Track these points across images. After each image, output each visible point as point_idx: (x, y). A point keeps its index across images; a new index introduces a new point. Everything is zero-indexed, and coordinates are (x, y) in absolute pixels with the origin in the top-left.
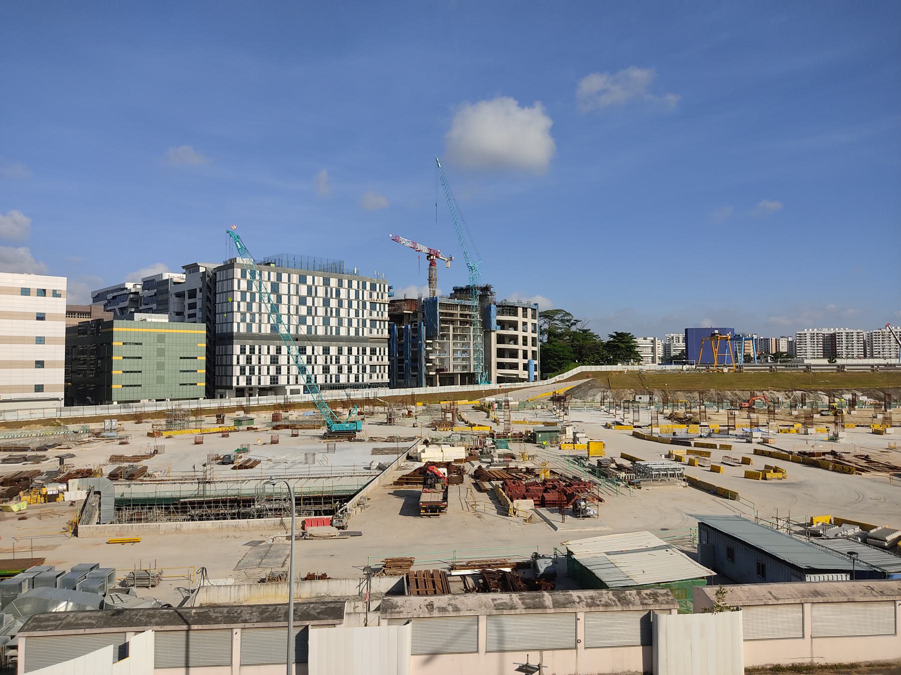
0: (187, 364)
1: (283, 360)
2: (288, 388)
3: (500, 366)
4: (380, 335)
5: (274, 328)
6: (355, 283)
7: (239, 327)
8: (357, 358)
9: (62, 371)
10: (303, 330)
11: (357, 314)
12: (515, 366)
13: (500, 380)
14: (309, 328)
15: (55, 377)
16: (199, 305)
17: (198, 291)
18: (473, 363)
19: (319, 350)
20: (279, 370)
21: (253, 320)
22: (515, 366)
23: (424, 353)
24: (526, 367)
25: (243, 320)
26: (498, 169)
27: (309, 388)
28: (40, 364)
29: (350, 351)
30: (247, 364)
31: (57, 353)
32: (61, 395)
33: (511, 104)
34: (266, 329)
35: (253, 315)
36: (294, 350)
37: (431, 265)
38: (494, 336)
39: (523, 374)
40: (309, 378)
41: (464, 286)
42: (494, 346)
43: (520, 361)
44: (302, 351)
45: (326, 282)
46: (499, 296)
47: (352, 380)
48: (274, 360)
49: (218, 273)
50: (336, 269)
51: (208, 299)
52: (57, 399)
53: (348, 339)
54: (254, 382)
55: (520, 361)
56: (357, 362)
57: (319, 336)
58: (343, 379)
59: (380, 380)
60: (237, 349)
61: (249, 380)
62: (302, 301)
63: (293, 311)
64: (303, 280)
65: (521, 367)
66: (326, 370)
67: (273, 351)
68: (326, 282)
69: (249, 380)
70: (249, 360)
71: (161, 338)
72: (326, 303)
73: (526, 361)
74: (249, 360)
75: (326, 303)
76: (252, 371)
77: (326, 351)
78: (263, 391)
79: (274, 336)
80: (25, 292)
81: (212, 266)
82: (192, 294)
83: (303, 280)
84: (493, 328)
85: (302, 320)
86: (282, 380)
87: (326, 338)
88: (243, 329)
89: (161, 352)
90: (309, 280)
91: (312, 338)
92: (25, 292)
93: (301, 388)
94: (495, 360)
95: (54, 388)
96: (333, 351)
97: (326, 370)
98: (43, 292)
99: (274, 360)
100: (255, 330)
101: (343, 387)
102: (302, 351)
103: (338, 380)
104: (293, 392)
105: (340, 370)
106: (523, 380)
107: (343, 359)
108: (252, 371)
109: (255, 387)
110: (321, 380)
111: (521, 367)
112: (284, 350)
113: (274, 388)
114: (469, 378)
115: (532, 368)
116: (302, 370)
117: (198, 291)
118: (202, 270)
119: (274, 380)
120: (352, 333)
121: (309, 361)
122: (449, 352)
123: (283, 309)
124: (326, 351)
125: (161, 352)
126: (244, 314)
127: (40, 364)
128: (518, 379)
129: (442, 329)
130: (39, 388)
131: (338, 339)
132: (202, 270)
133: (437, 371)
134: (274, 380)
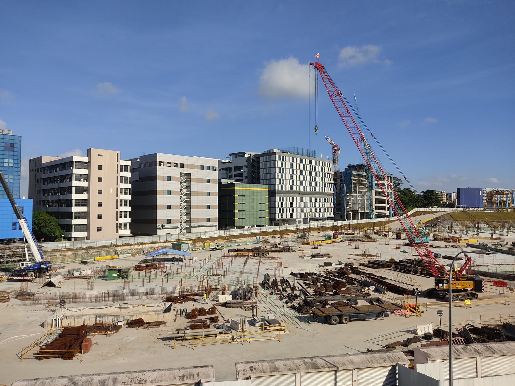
0: (262, 207)
1: (295, 205)
2: (297, 220)
3: (376, 208)
4: (330, 192)
5: (292, 188)
6: (321, 163)
7: (278, 188)
8: (322, 204)
9: (216, 211)
10: (302, 189)
11: (322, 181)
12: (384, 209)
13: (378, 216)
14: (304, 187)
15: (214, 213)
16: (245, 174)
17: (244, 167)
18: (366, 206)
19: (308, 199)
20: (293, 210)
21: (283, 183)
22: (384, 209)
23: (345, 201)
24: (389, 209)
25: (280, 183)
26: (287, 98)
27: (305, 221)
28: (208, 207)
29: (320, 201)
30: (285, 206)
31: (214, 201)
32: (216, 223)
33: (293, 62)
34: (288, 189)
35: (283, 180)
36: (299, 199)
37: (335, 152)
38: (373, 191)
39: (387, 213)
40: (305, 215)
41: (355, 164)
42: (374, 197)
43: (386, 206)
44: (302, 200)
45: (310, 163)
46: (375, 170)
47: (321, 216)
48: (292, 205)
49: (262, 158)
50: (311, 155)
51: (253, 172)
52: (216, 226)
53: (319, 194)
54: (284, 217)
55: (386, 206)
56: (322, 206)
57: (316, 192)
58: (317, 216)
59: (330, 216)
60: (278, 198)
61: (282, 215)
62: (302, 173)
63: (298, 179)
64: (302, 161)
65: (387, 209)
66: (311, 210)
67: (291, 201)
68: (310, 163)
69: (282, 215)
70: (282, 204)
71: (252, 192)
72: (311, 174)
73: (388, 206)
74: (282, 204)
75: (311, 174)
76: (283, 210)
77: (311, 200)
78: (285, 221)
79: (291, 192)
80: (202, 168)
81: (253, 154)
82: (238, 168)
83: (302, 161)
84: (374, 187)
85: (302, 184)
86: (295, 216)
87: (310, 193)
88: (280, 189)
89: (252, 200)
90: (304, 160)
91: (305, 193)
92: (202, 168)
93: (302, 220)
94: (374, 205)
95: (214, 220)
96: (314, 200)
97: (311, 210)
98: (208, 168)
99: (292, 205)
100: (284, 189)
101: (317, 220)
102: (302, 200)
103: (315, 216)
104: (299, 222)
105: (316, 209)
106: (388, 216)
107: (317, 206)
108: (283, 210)
109: (280, 220)
110: (309, 217)
111: (387, 209)
112: (295, 198)
113: (291, 221)
114: (363, 216)
115: (391, 209)
116: (302, 211)
117: (244, 167)
118: (246, 156)
119: (292, 215)
120: (321, 191)
121: (305, 206)
122: (357, 201)
123: (294, 177)
124: (311, 200)
125: (252, 200)
126: (280, 180)
127: (208, 207)
128: (384, 216)
129: (354, 187)
130: (208, 220)
131: (315, 193)
132: (246, 156)
133: (352, 211)
134: (292, 215)
